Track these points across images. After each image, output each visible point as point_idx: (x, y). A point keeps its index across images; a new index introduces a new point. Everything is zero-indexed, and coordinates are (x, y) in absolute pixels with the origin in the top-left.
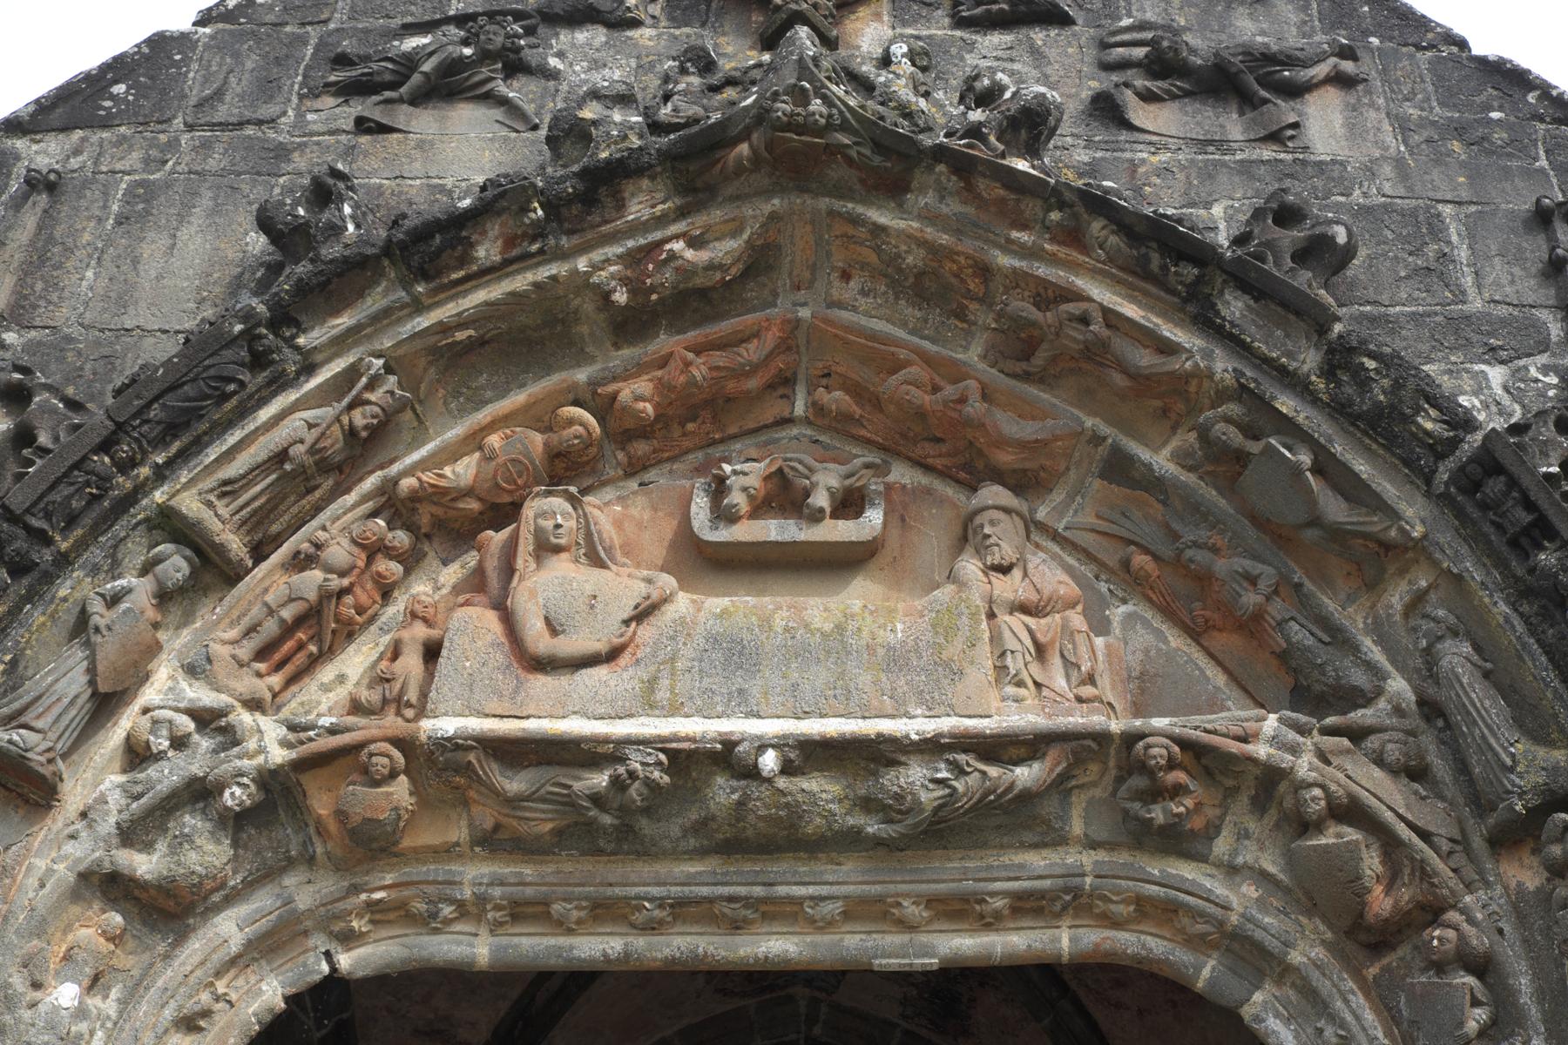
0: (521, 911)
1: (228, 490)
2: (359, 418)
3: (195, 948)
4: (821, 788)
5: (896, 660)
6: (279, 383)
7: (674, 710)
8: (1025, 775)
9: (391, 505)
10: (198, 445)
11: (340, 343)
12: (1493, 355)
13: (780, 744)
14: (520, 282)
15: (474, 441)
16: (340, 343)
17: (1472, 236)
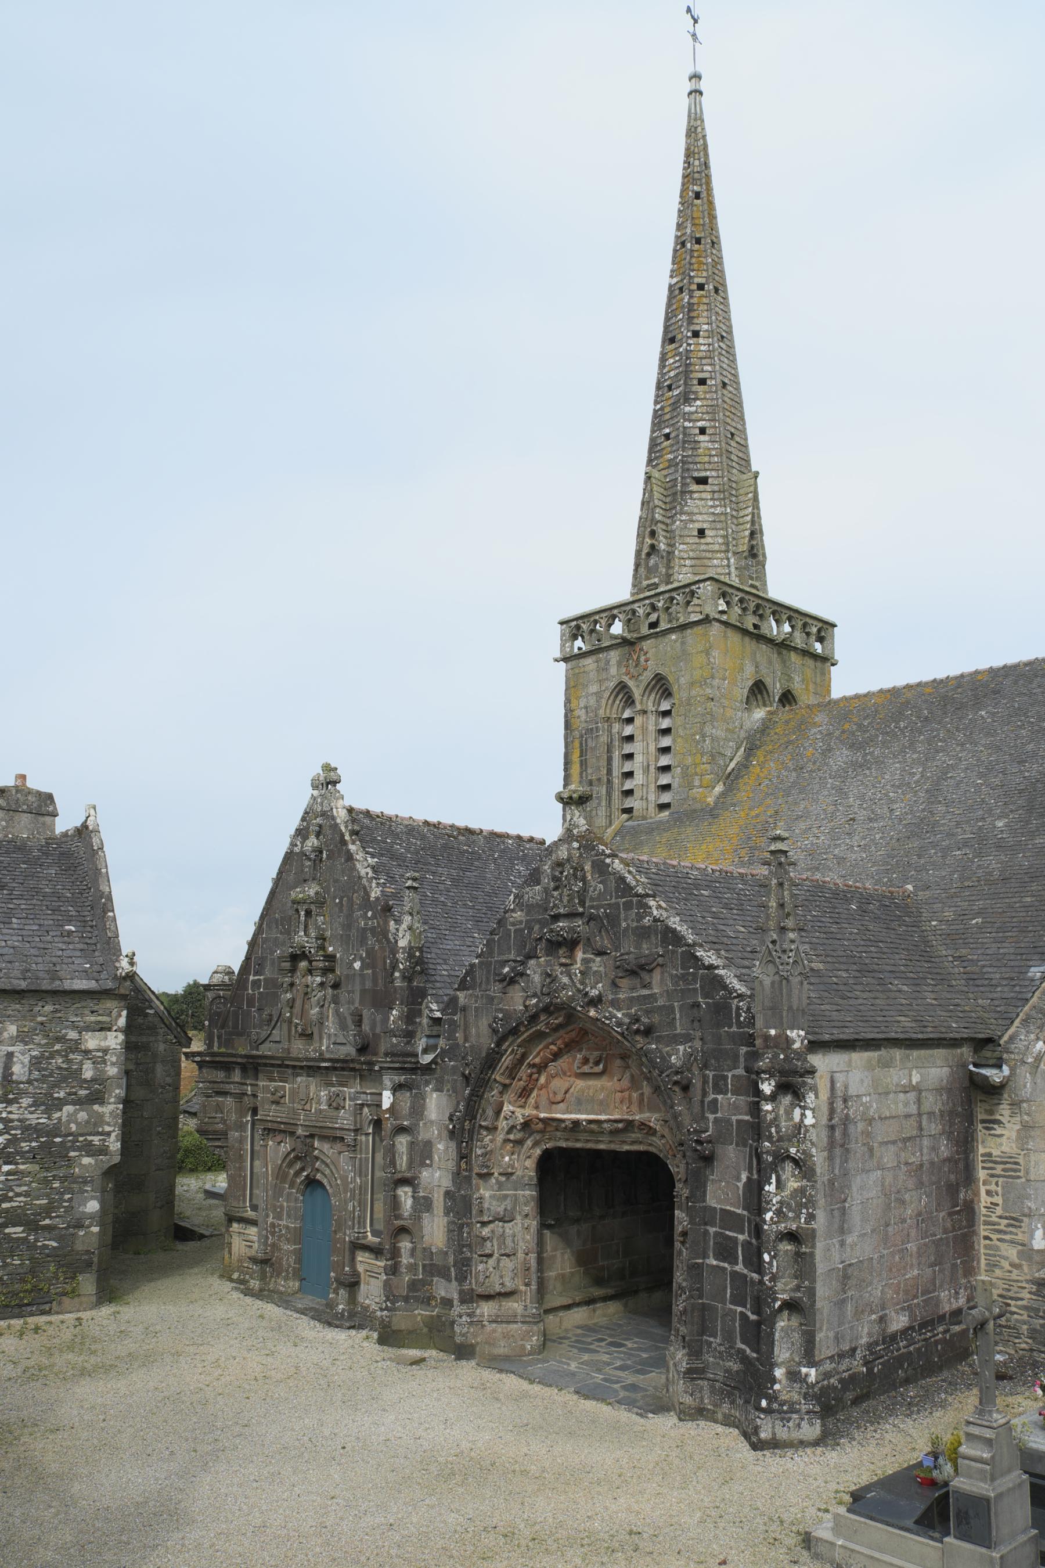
0: (567, 1140)
1: (502, 1074)
2: (518, 1057)
3: (525, 1146)
4: (593, 1126)
5: (601, 1103)
6: (502, 1055)
7: (571, 1113)
8: (620, 1125)
9: (530, 1066)
10: (495, 1068)
11: (509, 1046)
12: (681, 1043)
13: (585, 1120)
14: (531, 1031)
15: (538, 1053)
16: (509, 1046)
17: (681, 1011)
